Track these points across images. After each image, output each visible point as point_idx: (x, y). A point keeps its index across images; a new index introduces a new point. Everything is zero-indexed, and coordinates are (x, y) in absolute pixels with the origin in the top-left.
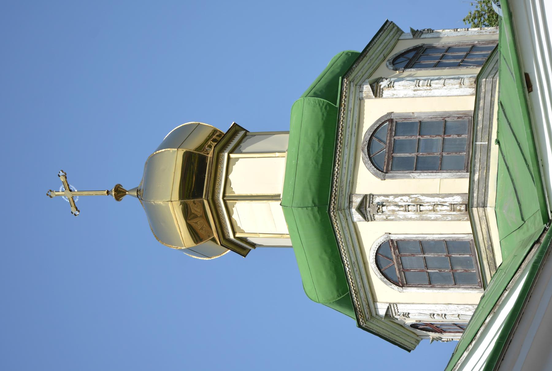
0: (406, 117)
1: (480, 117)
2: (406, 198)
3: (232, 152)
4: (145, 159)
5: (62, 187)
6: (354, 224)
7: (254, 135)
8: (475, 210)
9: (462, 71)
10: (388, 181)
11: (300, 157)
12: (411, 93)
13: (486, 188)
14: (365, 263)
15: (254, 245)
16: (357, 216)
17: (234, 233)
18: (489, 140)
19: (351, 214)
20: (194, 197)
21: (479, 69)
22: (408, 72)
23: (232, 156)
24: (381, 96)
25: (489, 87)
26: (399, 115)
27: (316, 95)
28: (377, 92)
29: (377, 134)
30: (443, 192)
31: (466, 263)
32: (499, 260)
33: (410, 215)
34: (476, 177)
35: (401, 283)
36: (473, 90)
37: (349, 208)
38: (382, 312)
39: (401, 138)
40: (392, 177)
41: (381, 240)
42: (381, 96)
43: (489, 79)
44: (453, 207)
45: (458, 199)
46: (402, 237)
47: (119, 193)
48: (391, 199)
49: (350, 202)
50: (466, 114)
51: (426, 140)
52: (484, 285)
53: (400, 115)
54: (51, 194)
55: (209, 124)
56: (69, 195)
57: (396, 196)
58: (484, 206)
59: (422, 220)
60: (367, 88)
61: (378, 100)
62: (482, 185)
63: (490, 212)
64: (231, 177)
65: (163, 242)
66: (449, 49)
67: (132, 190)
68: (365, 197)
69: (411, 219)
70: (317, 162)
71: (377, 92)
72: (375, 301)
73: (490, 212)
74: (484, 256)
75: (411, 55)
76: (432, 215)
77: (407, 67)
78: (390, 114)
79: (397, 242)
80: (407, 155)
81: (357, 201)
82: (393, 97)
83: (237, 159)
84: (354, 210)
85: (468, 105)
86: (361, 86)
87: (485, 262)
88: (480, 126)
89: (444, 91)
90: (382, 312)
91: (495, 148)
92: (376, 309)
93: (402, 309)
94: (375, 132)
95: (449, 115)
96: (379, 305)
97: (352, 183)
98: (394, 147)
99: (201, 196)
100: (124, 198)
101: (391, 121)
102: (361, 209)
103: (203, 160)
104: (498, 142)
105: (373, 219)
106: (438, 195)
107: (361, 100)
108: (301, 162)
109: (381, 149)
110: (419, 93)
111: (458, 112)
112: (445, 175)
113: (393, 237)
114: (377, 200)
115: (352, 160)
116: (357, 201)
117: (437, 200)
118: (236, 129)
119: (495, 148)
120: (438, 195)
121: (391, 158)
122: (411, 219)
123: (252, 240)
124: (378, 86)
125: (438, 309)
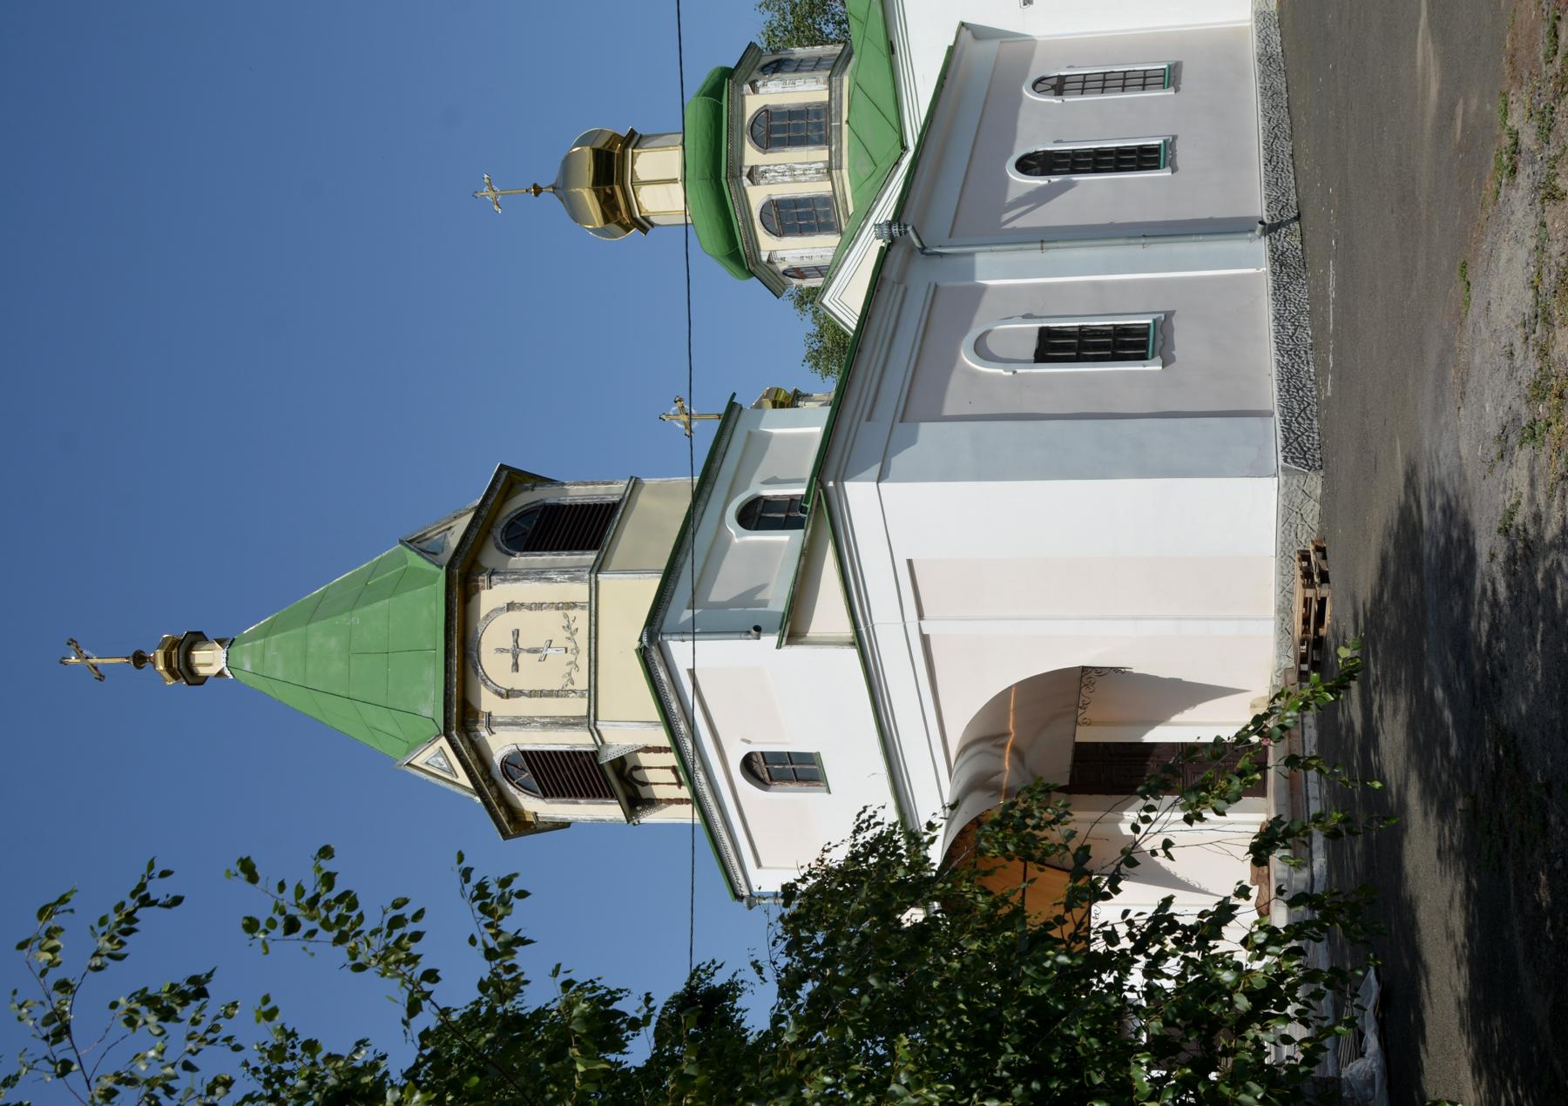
0: (777, 108)
1: (833, 105)
2: (783, 167)
3: (634, 148)
4: (562, 157)
5: (486, 189)
6: (744, 188)
7: (648, 136)
8: (834, 172)
9: (816, 73)
10: (768, 155)
11: (698, 142)
12: (780, 89)
13: (841, 156)
14: (752, 220)
15: (652, 225)
16: (746, 182)
17: (640, 212)
18: (841, 122)
19: (742, 181)
20: (607, 184)
21: (829, 72)
22: (775, 76)
23: (635, 151)
24: (758, 93)
25: (838, 83)
26: (773, 106)
27: (704, 95)
28: (755, 90)
29: (758, 121)
30: (810, 160)
31: (826, 214)
32: (851, 210)
33: (787, 179)
34: (833, 148)
35: (780, 234)
36: (826, 86)
37: (741, 176)
38: (765, 258)
39: (776, 123)
40: (771, 152)
41: (765, 200)
42: (758, 93)
43: (838, 78)
44: (818, 171)
45: (821, 165)
46: (780, 197)
47: (538, 190)
48: (771, 167)
49: (741, 172)
50: (822, 103)
51: (794, 124)
52: (840, 232)
53: (774, 107)
54: (478, 195)
55: (610, 129)
56: (492, 194)
57: (775, 165)
58: (841, 168)
59: (796, 182)
60: (747, 87)
61: (756, 96)
62: (838, 153)
63: (845, 172)
64: (635, 167)
65: (576, 221)
66: (802, 60)
67: (549, 187)
68: (752, 167)
69: (787, 182)
70: (711, 145)
71: (755, 90)
72: (759, 250)
73: (845, 172)
74: (840, 207)
75: (774, 65)
76: (803, 178)
77: (773, 73)
78: (765, 106)
79: (777, 201)
80: (781, 135)
81: (746, 171)
82: (767, 93)
83: (639, 153)
84: (744, 178)
85: (824, 97)
86: (742, 86)
87: (841, 213)
88: (833, 112)
89: (805, 88)
90: (765, 258)
91: (845, 127)
92: (760, 256)
93: (780, 254)
94: (755, 120)
95: (810, 104)
96: (762, 253)
97: (741, 158)
98: (770, 130)
99: (612, 183)
100: (541, 195)
101: (767, 111)
102: (750, 176)
103: (610, 155)
104: (847, 122)
105: (758, 184)
106: (806, 163)
107: (743, 96)
108: (699, 146)
109: (759, 130)
110: (786, 90)
111: (816, 103)
112: (811, 148)
113: (774, 198)
114: (761, 169)
115: (740, 141)
116: (746, 171)
117: (805, 166)
118: (632, 133)
119: (845, 127)
120: (806, 163)
121: (769, 138)
122: (787, 182)
123: (653, 219)
124: (755, 85)
125: (806, 253)
